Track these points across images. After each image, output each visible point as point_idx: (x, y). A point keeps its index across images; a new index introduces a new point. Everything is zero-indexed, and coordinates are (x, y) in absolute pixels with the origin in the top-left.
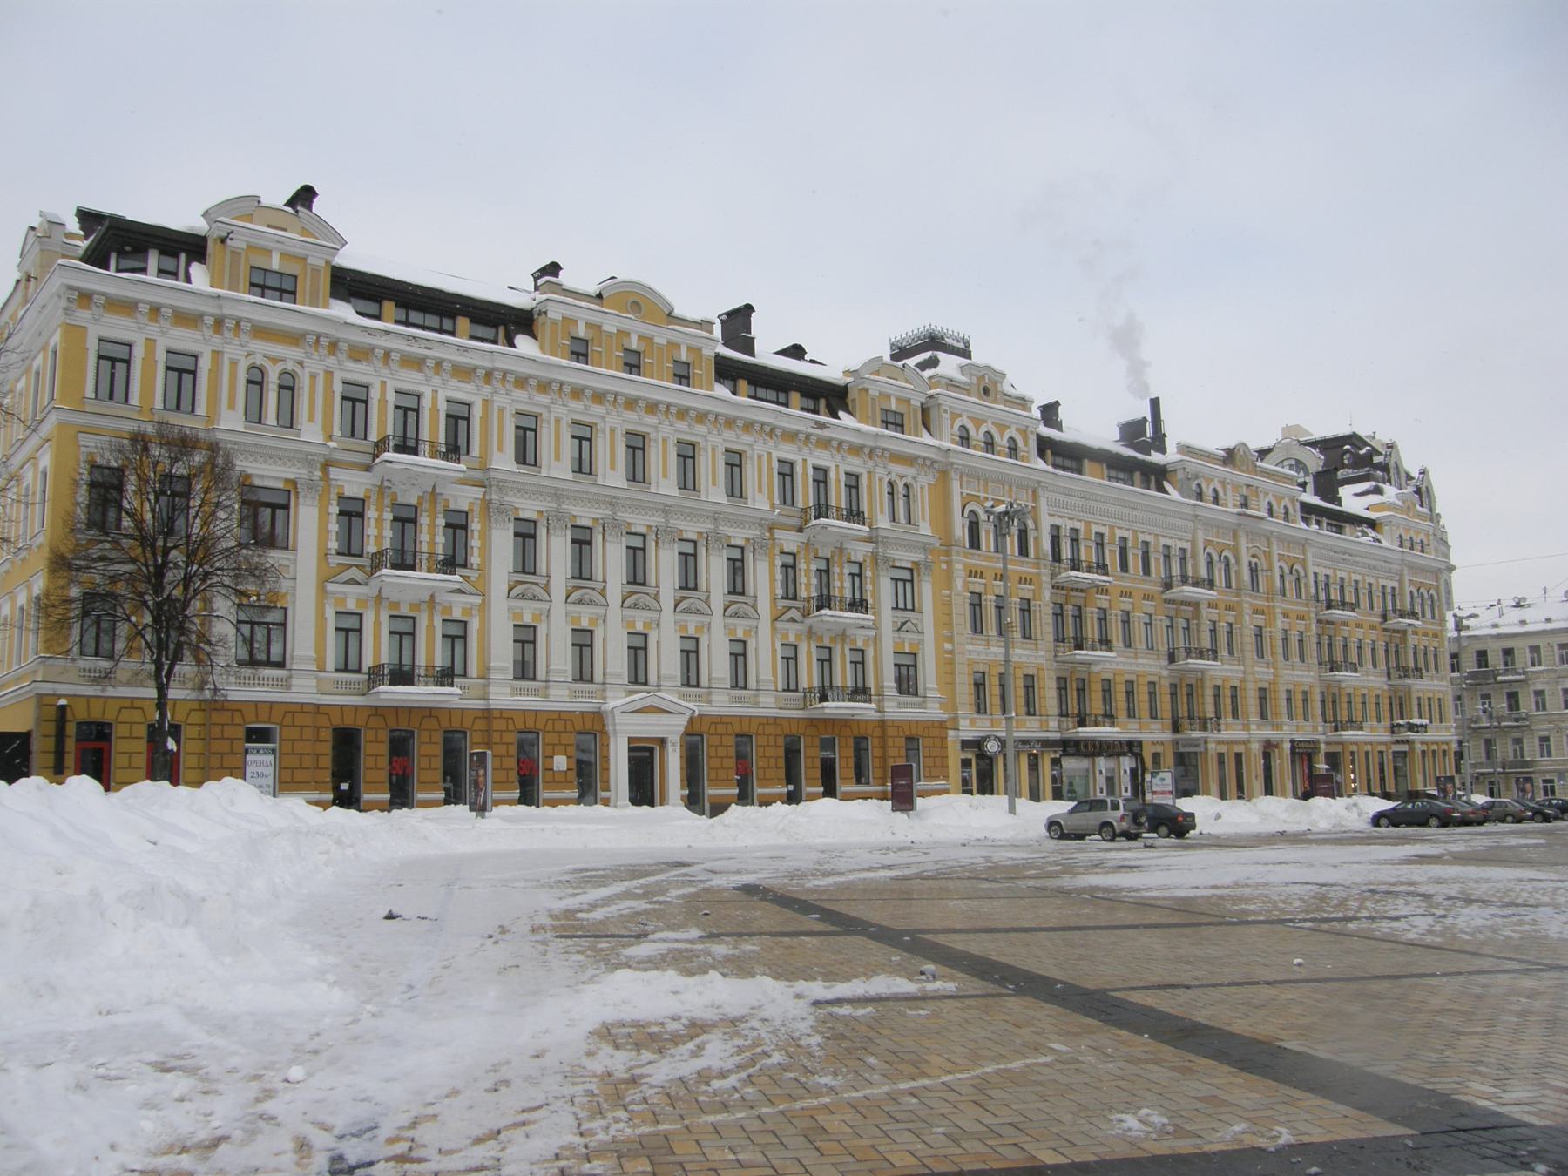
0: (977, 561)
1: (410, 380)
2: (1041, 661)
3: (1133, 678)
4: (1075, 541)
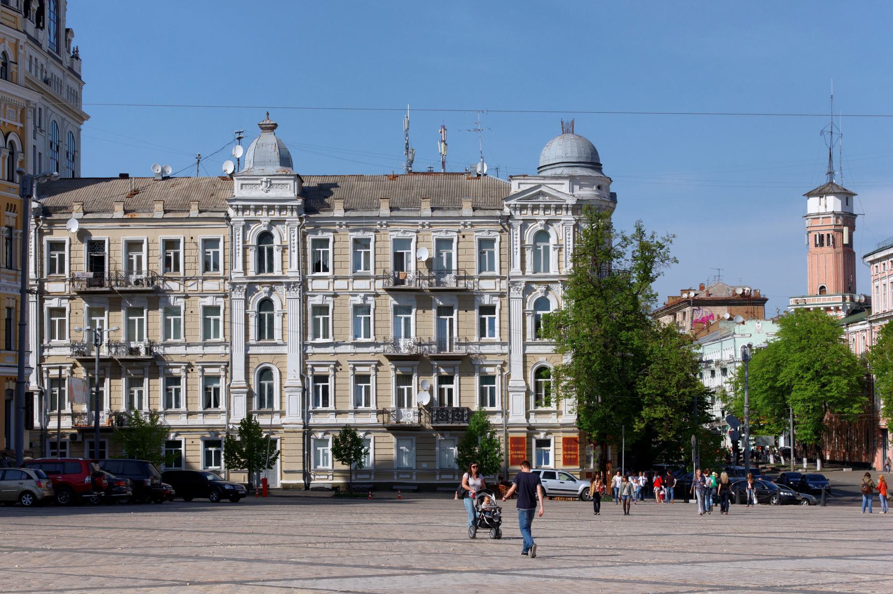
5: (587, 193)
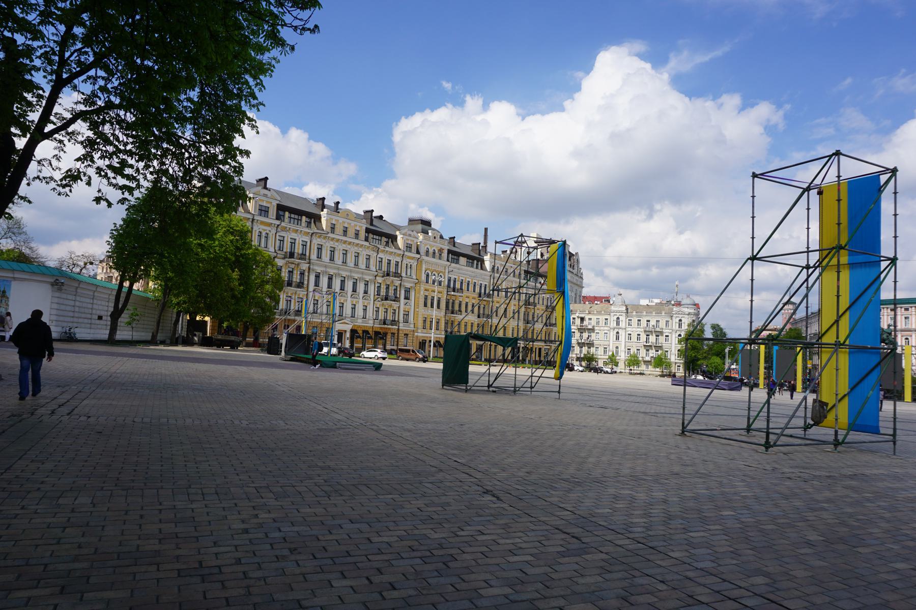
1: (294, 235)
4: (455, 281)
5: (692, 311)
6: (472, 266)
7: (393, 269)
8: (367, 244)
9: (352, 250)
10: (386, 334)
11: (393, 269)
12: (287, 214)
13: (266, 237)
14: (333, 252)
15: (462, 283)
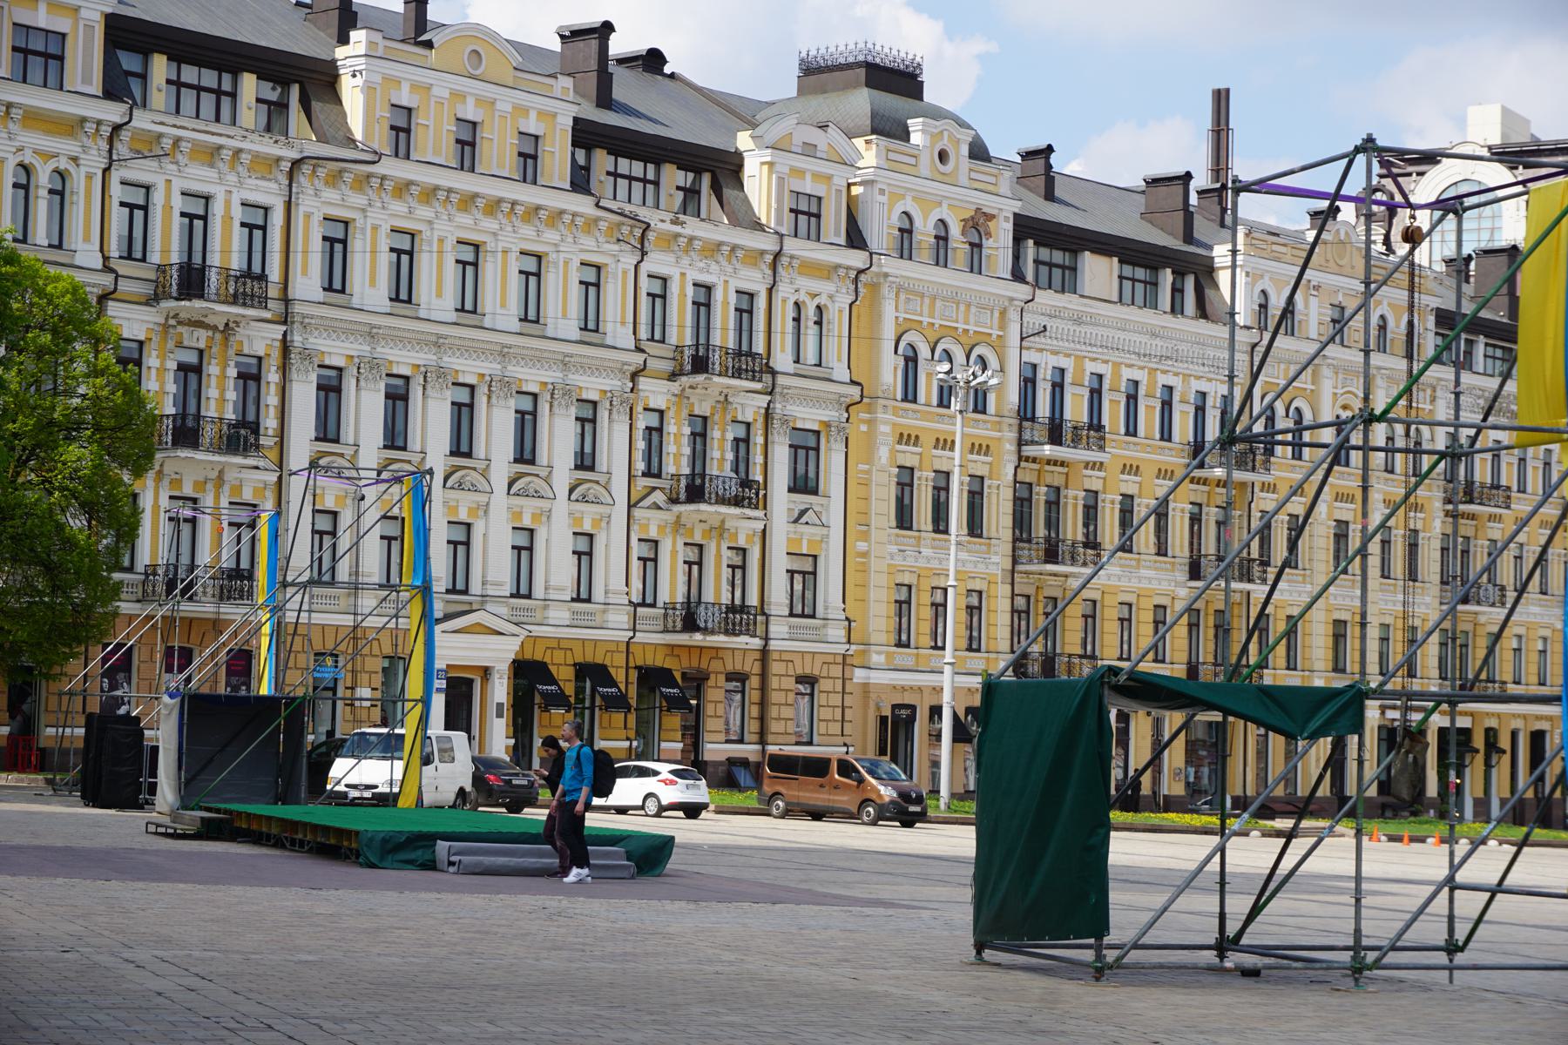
0: (911, 421)
1: (200, 177)
2: (993, 569)
3: (1131, 598)
4: (1058, 387)
6: (1151, 303)
7: (723, 334)
8: (581, 204)
9: (506, 245)
10: (697, 681)
11: (723, 334)
12: (160, 67)
13: (59, 194)
14: (405, 255)
15: (1096, 394)
